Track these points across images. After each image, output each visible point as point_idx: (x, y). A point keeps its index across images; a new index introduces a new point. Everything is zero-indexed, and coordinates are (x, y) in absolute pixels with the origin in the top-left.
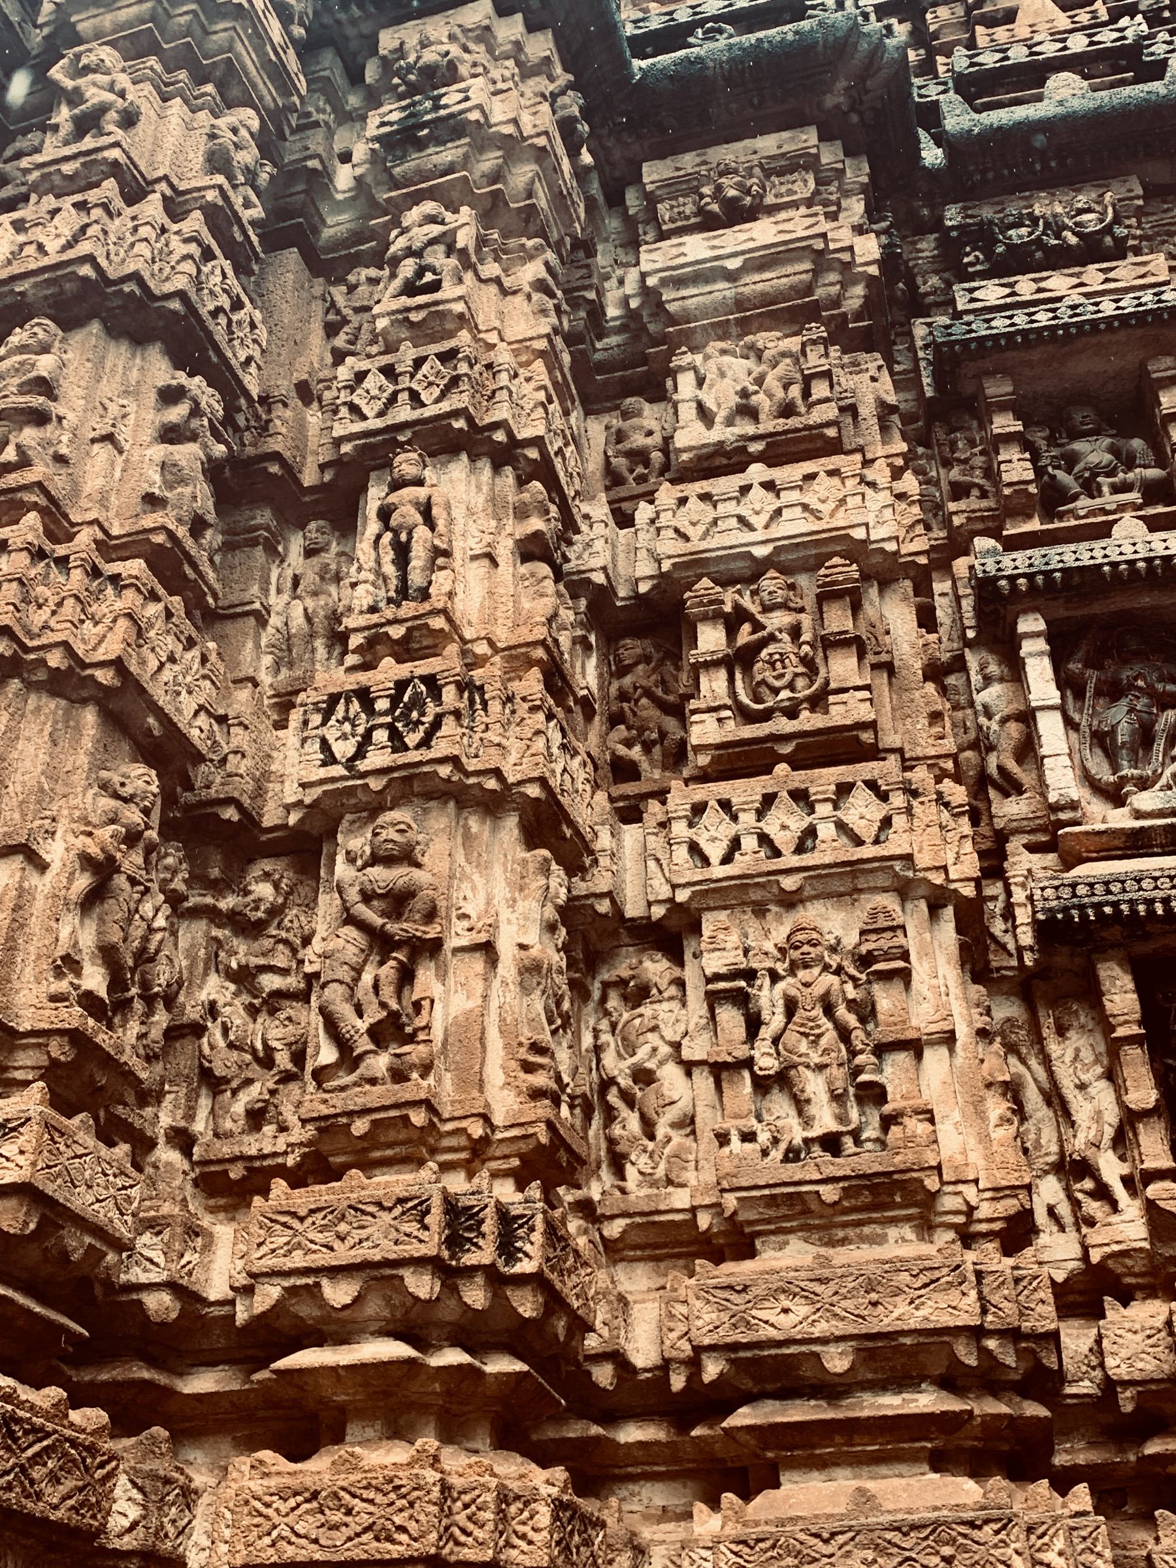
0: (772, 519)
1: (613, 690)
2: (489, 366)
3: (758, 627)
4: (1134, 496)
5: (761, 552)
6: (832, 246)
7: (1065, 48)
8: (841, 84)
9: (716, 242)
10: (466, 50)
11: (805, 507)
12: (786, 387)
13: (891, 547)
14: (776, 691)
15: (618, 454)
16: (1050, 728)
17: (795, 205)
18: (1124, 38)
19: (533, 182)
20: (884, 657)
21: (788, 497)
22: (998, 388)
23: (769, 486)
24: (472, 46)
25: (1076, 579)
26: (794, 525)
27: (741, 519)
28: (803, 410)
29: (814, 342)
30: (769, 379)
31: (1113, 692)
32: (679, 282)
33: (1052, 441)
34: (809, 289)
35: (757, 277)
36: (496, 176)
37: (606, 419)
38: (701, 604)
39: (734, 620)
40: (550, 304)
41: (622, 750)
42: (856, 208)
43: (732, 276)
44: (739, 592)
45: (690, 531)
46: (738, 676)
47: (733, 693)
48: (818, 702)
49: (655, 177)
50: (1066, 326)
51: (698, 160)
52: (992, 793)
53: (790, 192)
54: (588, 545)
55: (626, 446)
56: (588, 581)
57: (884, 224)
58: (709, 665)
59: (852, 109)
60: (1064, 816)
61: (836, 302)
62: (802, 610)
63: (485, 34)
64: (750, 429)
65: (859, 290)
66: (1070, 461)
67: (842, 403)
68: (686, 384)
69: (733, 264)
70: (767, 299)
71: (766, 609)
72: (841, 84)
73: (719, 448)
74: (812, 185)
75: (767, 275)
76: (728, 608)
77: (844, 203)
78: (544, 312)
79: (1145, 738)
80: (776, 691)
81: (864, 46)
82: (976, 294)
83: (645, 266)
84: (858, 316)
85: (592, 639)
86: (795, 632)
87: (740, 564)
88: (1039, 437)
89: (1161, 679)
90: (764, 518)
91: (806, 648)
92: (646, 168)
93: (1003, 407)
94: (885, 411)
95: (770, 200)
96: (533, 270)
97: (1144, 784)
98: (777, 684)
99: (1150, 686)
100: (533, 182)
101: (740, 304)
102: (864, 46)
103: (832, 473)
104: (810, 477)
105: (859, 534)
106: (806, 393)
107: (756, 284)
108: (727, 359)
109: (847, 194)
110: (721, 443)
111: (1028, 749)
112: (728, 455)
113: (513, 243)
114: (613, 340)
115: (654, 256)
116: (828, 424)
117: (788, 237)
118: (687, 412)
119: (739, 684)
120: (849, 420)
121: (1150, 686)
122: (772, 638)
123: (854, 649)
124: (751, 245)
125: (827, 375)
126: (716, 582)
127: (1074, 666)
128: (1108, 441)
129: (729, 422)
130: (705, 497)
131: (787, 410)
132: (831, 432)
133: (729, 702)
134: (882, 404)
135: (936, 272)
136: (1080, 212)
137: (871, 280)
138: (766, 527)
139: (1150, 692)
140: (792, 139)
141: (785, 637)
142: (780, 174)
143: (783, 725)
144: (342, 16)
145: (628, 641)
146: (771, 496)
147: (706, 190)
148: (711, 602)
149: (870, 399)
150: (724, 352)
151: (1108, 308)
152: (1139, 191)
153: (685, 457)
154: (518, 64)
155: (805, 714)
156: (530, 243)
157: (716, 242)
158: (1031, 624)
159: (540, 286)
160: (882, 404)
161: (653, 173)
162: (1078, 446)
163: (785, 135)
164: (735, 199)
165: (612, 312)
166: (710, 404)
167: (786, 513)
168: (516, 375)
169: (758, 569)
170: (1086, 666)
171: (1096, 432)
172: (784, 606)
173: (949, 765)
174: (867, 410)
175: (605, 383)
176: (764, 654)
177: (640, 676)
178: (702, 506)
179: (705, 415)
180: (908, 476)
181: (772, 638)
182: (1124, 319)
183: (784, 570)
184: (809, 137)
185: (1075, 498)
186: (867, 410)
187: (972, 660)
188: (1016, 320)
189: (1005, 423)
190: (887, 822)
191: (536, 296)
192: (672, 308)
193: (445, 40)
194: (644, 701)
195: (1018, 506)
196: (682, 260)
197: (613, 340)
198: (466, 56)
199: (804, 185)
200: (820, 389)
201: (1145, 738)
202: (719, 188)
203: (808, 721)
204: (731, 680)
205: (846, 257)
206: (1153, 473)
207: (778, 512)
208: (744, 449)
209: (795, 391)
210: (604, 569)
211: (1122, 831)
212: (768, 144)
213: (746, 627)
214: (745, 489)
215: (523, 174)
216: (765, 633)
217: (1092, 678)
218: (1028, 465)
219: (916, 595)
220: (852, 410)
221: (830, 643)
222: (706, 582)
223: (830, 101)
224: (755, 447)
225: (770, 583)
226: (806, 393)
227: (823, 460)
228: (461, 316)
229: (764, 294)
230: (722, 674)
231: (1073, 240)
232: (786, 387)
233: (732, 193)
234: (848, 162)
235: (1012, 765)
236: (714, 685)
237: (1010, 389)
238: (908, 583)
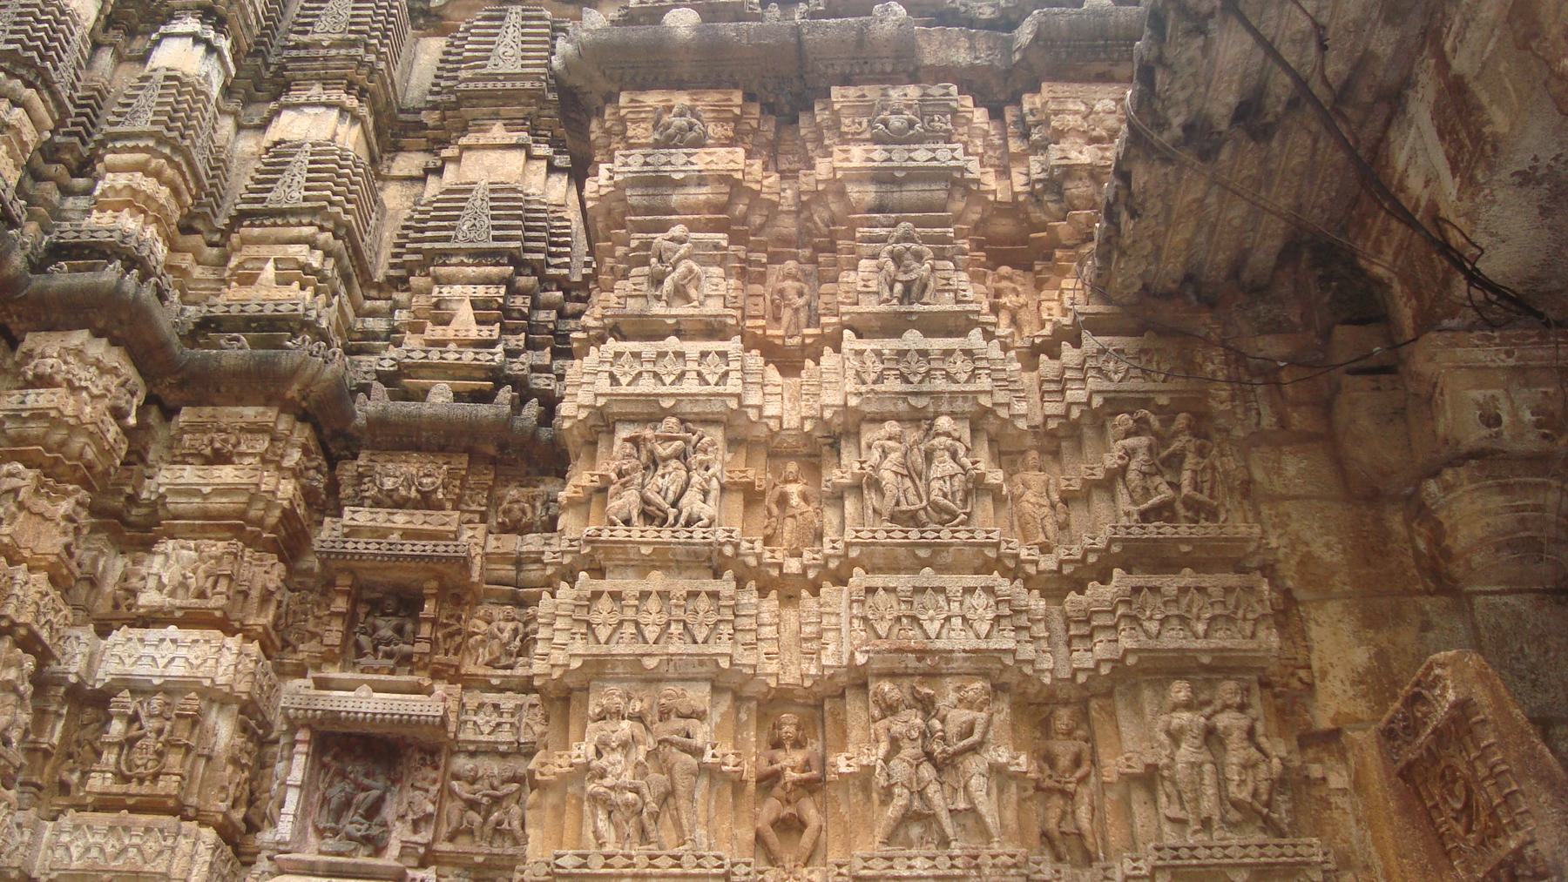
0: (169, 662)
1: (74, 738)
2: (12, 578)
3: (141, 728)
4: (391, 663)
5: (157, 681)
6: (263, 487)
7: (459, 359)
8: (296, 387)
9: (201, 473)
10: (66, 362)
11: (187, 659)
12: (207, 577)
13: (227, 689)
14: (138, 767)
15: (121, 589)
16: (292, 797)
17: (253, 455)
18: (493, 360)
19: (83, 448)
20: (206, 752)
21: (183, 652)
22: (344, 581)
23: (174, 641)
24: (70, 359)
25: (329, 716)
26: (178, 670)
27: (154, 659)
28: (210, 595)
29: (229, 553)
30: (200, 570)
31: (343, 775)
32: (178, 493)
33: (367, 615)
34: (242, 515)
35: (218, 500)
36: (63, 444)
37: (126, 560)
38: (118, 707)
39: (134, 719)
40: (71, 526)
41: (65, 775)
42: (294, 457)
43: (205, 497)
44: (140, 702)
45: (127, 661)
46: (125, 752)
47: (118, 762)
48: (155, 777)
49: (186, 418)
50: (383, 555)
51: (212, 413)
52: (266, 822)
53: (253, 447)
54: (74, 657)
55: (126, 585)
56: (67, 679)
57: (315, 464)
58: (111, 744)
59: (304, 398)
60: (282, 848)
61: (260, 522)
62: (168, 719)
63: (79, 353)
64: (178, 602)
65: (277, 513)
66: (375, 629)
67: (240, 588)
68: (159, 560)
69: (207, 490)
70: (222, 516)
71: (151, 716)
72: (296, 387)
73: (160, 609)
74: (266, 444)
75: (224, 500)
76: (130, 712)
77: (289, 451)
78: (65, 533)
79: (347, 804)
80: (138, 767)
81: (309, 371)
82: (356, 516)
83: (160, 479)
84: (274, 529)
85: (65, 711)
86: (160, 732)
87: (147, 685)
88: (362, 610)
89: (367, 775)
90: (166, 660)
91: (159, 745)
92: (184, 410)
93: (343, 593)
94: (266, 596)
95: (243, 448)
96: (65, 506)
97: (336, 833)
98: (139, 762)
99: (356, 778)
100: (83, 448)
101: (206, 515)
102: (309, 371)
103: (208, 642)
104: (197, 641)
105: (207, 683)
106: (215, 585)
107: (218, 503)
108: (185, 552)
109: (293, 446)
110: (161, 607)
111: (282, 805)
112: (165, 613)
113: (61, 486)
114: (144, 511)
115: (167, 474)
116: (216, 609)
117: (237, 480)
118: (152, 582)
119: (123, 757)
120: (240, 598)
121: (356, 778)
122: (144, 735)
123: (183, 750)
124: (217, 481)
125: (230, 577)
126: (131, 692)
127: (327, 759)
128: (394, 621)
129: (172, 594)
130: (141, 640)
131: (202, 594)
132: (218, 614)
133: (113, 769)
134: (265, 588)
135: (353, 486)
136: (426, 475)
137: (284, 511)
138: (165, 666)
139: (355, 782)
140: (264, 414)
141: (153, 735)
142: (250, 431)
143: (133, 788)
144: (8, 320)
145: (89, 710)
146: (173, 647)
147: (206, 440)
148: (124, 707)
149: (259, 585)
150: (182, 547)
151: (407, 550)
152: (465, 466)
153: (142, 610)
154: (98, 368)
155: (147, 783)
156: (70, 488)
157: (201, 473)
158: (302, 735)
159: (69, 518)
160: (265, 588)
161: (185, 416)
162: (380, 622)
163: (261, 409)
164: (218, 449)
165: (145, 495)
166: (165, 580)
167: (177, 661)
168: (26, 583)
169: (156, 690)
170: (335, 758)
171: (393, 614)
172: (160, 715)
173: (220, 818)
174: (255, 593)
175: (131, 538)
176: (139, 743)
177: (87, 734)
178: (139, 646)
179: (160, 587)
180: (256, 643)
181: (144, 735)
182: (413, 557)
183: (167, 692)
184: (269, 415)
185: (365, 655)
186: (255, 593)
187: (282, 742)
188: (359, 546)
189: (341, 604)
190: (160, 853)
191: (63, 523)
192: (171, 507)
193: (55, 355)
194: (87, 747)
195: (329, 658)
196: (178, 481)
197: (144, 511)
198: (64, 367)
199: (263, 444)
200: (223, 586)
201: (347, 804)
202: (212, 441)
203: (146, 788)
204: (120, 755)
205: (269, 496)
206: (407, 648)
207: (173, 659)
208: (172, 612)
209: (211, 579)
210: (77, 673)
211: (300, 861)
212: (250, 413)
213: (137, 725)
214: (162, 640)
215: (78, 442)
216: (142, 732)
217: (335, 765)
218: (340, 635)
219: (241, 712)
220: (246, 594)
221: (171, 744)
222: (126, 693)
223: (289, 394)
224: (178, 614)
225: (157, 702)
226: (215, 585)
227: (206, 632)
228: (6, 545)
229: (219, 510)
230: (116, 750)
231: (413, 494)
232: (207, 577)
233: (217, 445)
234: (298, 425)
235: (275, 811)
236: (110, 757)
237: (349, 583)
238: (235, 707)
